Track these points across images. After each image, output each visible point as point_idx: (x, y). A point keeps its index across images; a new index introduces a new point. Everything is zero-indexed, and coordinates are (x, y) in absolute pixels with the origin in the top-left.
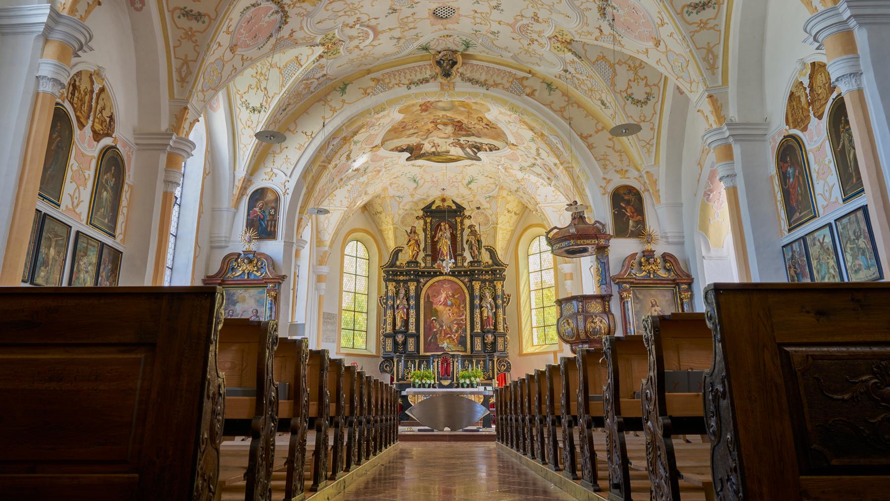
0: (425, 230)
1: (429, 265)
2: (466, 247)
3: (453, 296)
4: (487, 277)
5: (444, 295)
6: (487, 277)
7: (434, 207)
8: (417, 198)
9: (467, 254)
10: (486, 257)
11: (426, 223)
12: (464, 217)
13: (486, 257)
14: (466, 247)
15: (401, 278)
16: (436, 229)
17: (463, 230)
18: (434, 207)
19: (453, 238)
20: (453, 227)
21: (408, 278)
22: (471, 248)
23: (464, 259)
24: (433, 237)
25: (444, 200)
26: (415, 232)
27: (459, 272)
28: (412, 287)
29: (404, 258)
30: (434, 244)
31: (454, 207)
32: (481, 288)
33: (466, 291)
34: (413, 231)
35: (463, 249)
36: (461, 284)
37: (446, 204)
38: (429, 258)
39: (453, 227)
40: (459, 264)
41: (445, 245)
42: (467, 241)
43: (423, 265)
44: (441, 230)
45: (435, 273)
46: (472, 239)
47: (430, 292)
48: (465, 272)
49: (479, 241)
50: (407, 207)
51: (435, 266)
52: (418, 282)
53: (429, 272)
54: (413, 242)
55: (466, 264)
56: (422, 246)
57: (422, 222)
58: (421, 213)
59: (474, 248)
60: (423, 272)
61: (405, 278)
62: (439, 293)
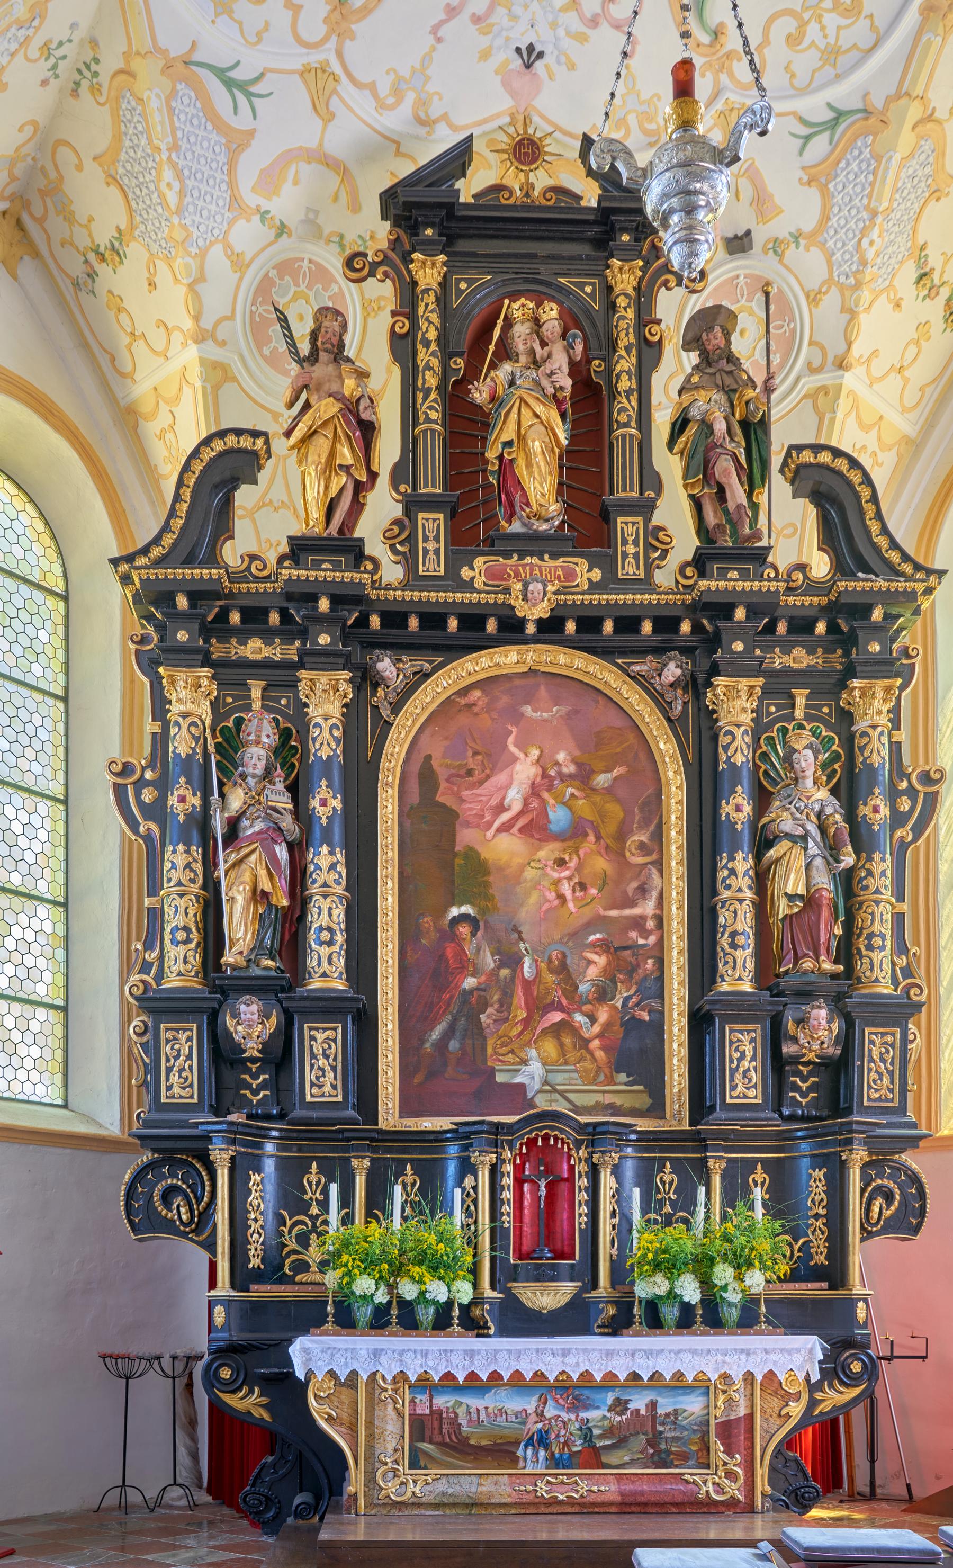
0: (403, 346)
1: (432, 564)
2: (669, 465)
3: (583, 776)
4: (800, 658)
5: (524, 771)
6: (800, 658)
7: (467, 189)
8: (358, 117)
9: (675, 513)
10: (791, 533)
11: (409, 296)
12: (657, 273)
13: (791, 533)
14: (669, 465)
15: (254, 649)
16: (477, 342)
17: (649, 352)
18: (467, 189)
19: (588, 401)
20: (592, 329)
21: (291, 652)
22: (701, 467)
23: (656, 542)
24: (455, 396)
25: (527, 151)
26: (338, 353)
27: (628, 623)
28: (325, 700)
29: (268, 521)
30: (467, 425)
31: (590, 194)
32: (759, 729)
33: (665, 746)
34: (327, 345)
35: (650, 480)
36: (635, 700)
37: (541, 180)
38: (432, 523)
39: (592, 329)
40: (629, 569)
41: (533, 445)
42: (680, 425)
43: (392, 572)
44: (505, 352)
45: (472, 621)
46: (710, 404)
47: (435, 748)
48: (666, 623)
49: (754, 430)
50: (287, 203)
51: (477, 571)
52: (366, 680)
53: (433, 619)
54: (327, 408)
55: (664, 577)
56: (388, 449)
57: (382, 290)
58: (376, 232)
59: (725, 469)
60: (395, 618)
61: (276, 652)
62: (495, 758)
